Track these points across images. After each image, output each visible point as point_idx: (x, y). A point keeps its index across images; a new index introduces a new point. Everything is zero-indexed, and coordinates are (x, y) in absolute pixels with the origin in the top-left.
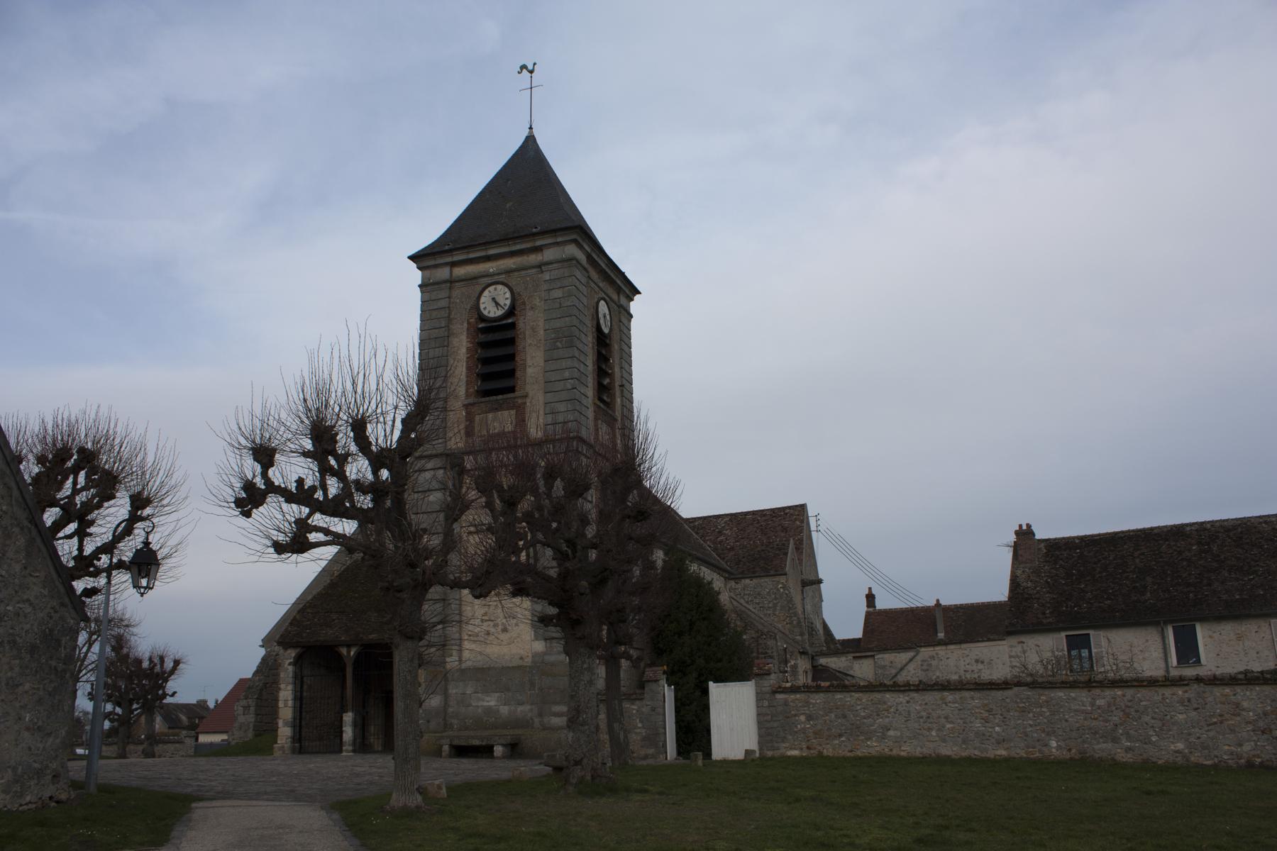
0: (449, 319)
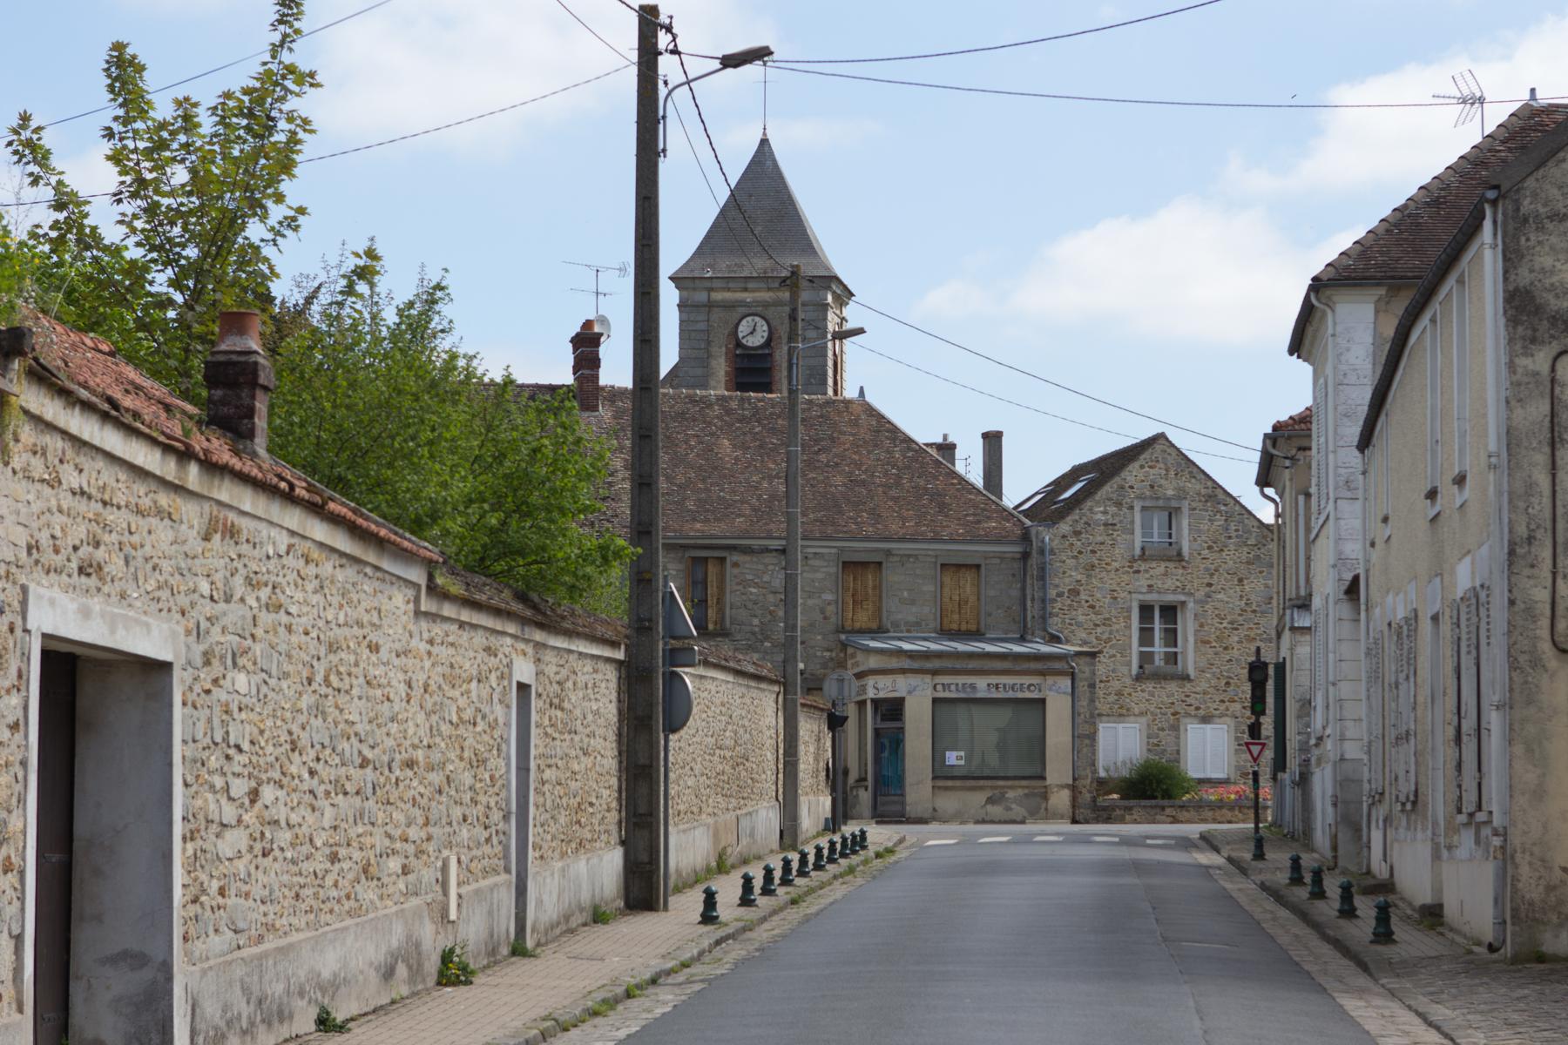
0: (709, 343)
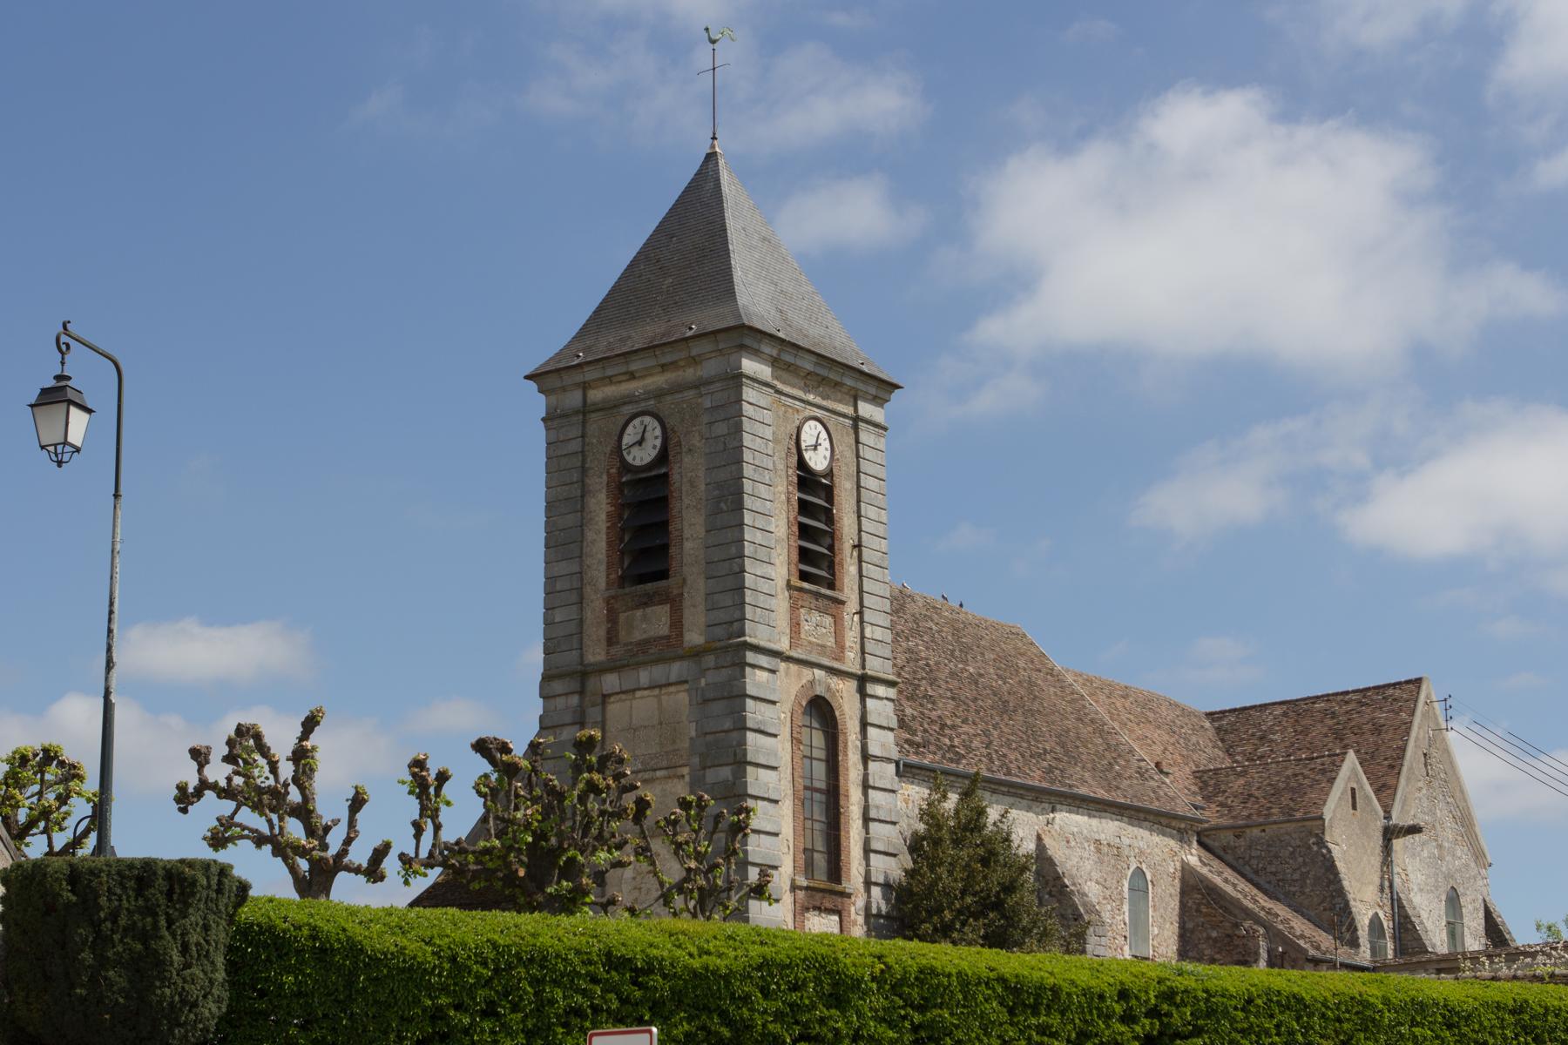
0: (584, 470)
